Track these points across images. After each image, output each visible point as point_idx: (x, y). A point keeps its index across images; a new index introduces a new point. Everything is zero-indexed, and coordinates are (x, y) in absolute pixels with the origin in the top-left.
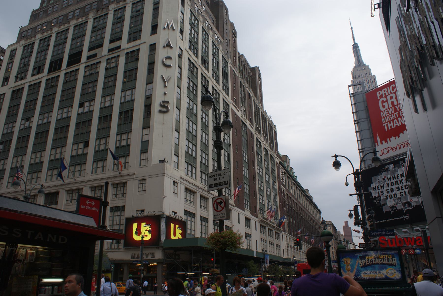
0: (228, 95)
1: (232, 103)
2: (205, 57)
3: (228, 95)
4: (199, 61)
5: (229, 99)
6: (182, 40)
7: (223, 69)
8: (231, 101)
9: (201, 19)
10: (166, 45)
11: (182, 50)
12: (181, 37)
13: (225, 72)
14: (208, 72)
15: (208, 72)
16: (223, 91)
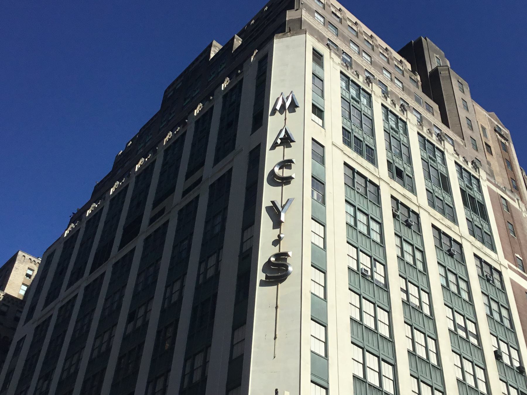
0: (493, 248)
1: (510, 268)
2: (399, 164)
3: (493, 248)
4: (380, 173)
5: (498, 258)
6: (323, 126)
7: (463, 192)
8: (506, 263)
9: (376, 90)
10: (279, 141)
11: (323, 147)
12: (320, 121)
13: (472, 199)
14: (416, 195)
15: (416, 195)
16: (472, 238)
